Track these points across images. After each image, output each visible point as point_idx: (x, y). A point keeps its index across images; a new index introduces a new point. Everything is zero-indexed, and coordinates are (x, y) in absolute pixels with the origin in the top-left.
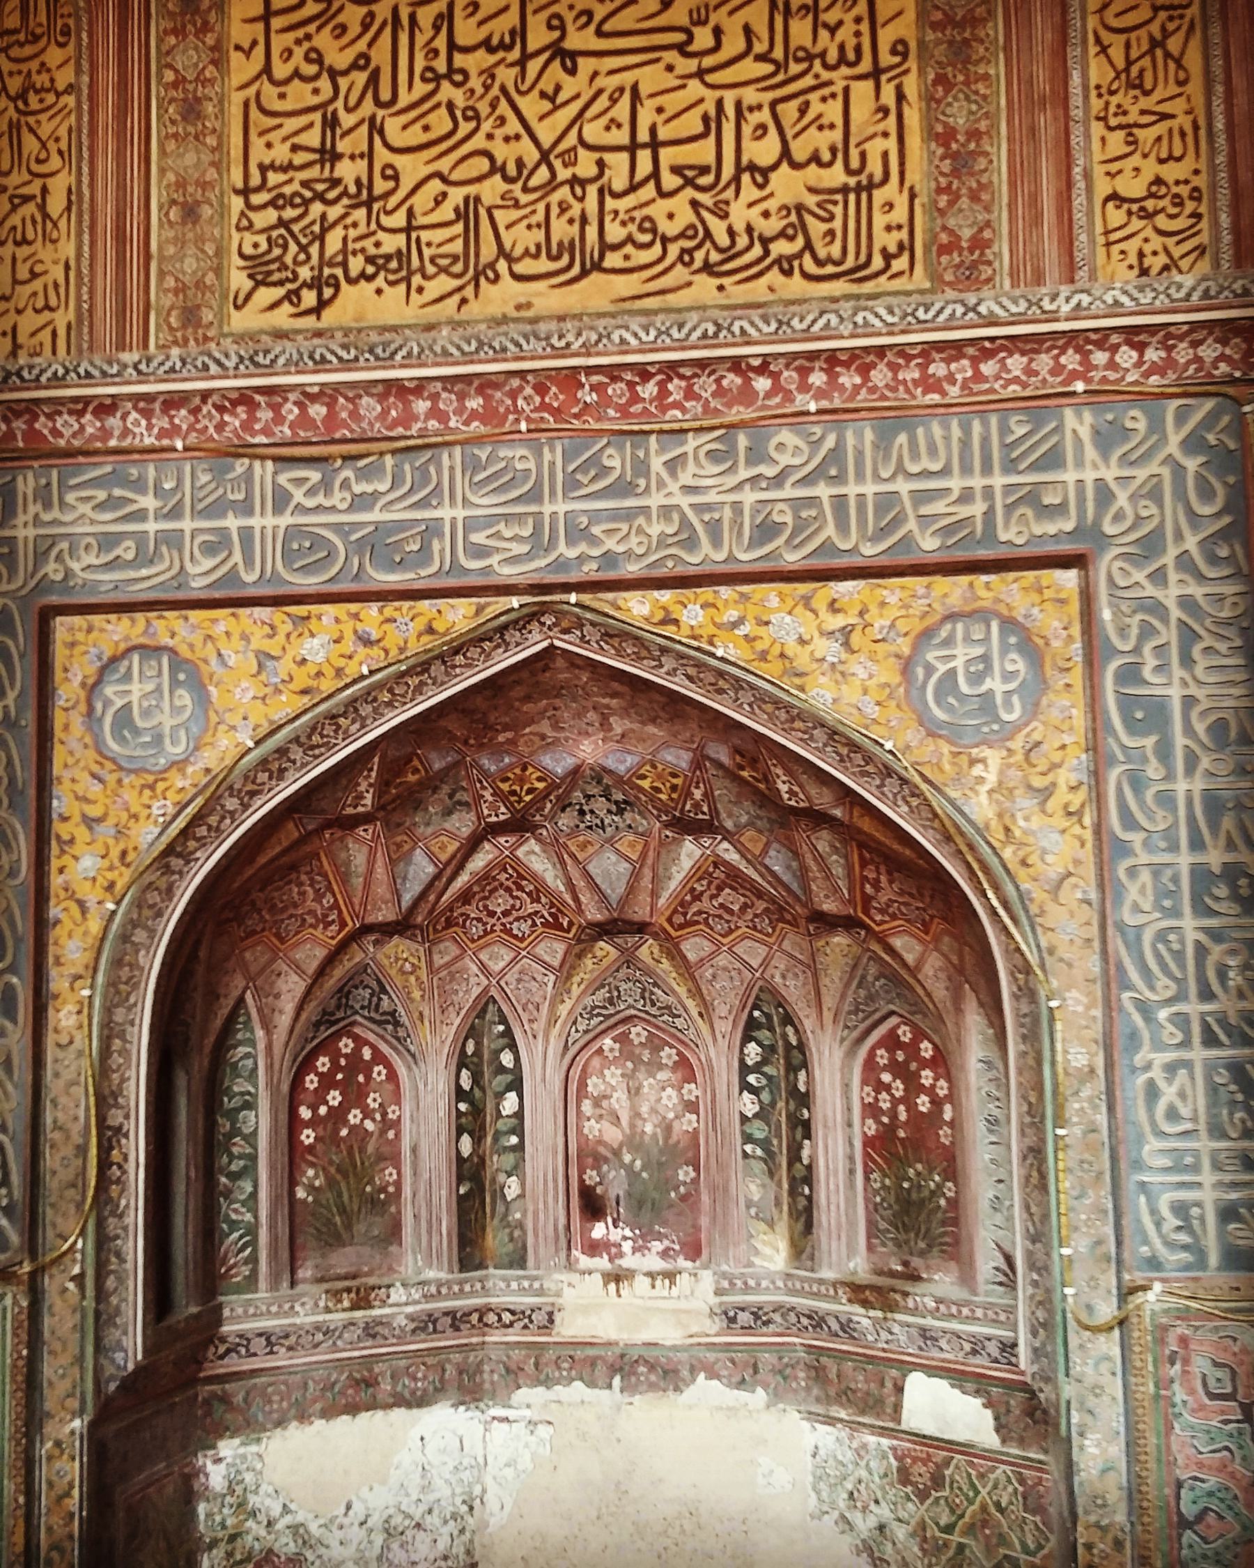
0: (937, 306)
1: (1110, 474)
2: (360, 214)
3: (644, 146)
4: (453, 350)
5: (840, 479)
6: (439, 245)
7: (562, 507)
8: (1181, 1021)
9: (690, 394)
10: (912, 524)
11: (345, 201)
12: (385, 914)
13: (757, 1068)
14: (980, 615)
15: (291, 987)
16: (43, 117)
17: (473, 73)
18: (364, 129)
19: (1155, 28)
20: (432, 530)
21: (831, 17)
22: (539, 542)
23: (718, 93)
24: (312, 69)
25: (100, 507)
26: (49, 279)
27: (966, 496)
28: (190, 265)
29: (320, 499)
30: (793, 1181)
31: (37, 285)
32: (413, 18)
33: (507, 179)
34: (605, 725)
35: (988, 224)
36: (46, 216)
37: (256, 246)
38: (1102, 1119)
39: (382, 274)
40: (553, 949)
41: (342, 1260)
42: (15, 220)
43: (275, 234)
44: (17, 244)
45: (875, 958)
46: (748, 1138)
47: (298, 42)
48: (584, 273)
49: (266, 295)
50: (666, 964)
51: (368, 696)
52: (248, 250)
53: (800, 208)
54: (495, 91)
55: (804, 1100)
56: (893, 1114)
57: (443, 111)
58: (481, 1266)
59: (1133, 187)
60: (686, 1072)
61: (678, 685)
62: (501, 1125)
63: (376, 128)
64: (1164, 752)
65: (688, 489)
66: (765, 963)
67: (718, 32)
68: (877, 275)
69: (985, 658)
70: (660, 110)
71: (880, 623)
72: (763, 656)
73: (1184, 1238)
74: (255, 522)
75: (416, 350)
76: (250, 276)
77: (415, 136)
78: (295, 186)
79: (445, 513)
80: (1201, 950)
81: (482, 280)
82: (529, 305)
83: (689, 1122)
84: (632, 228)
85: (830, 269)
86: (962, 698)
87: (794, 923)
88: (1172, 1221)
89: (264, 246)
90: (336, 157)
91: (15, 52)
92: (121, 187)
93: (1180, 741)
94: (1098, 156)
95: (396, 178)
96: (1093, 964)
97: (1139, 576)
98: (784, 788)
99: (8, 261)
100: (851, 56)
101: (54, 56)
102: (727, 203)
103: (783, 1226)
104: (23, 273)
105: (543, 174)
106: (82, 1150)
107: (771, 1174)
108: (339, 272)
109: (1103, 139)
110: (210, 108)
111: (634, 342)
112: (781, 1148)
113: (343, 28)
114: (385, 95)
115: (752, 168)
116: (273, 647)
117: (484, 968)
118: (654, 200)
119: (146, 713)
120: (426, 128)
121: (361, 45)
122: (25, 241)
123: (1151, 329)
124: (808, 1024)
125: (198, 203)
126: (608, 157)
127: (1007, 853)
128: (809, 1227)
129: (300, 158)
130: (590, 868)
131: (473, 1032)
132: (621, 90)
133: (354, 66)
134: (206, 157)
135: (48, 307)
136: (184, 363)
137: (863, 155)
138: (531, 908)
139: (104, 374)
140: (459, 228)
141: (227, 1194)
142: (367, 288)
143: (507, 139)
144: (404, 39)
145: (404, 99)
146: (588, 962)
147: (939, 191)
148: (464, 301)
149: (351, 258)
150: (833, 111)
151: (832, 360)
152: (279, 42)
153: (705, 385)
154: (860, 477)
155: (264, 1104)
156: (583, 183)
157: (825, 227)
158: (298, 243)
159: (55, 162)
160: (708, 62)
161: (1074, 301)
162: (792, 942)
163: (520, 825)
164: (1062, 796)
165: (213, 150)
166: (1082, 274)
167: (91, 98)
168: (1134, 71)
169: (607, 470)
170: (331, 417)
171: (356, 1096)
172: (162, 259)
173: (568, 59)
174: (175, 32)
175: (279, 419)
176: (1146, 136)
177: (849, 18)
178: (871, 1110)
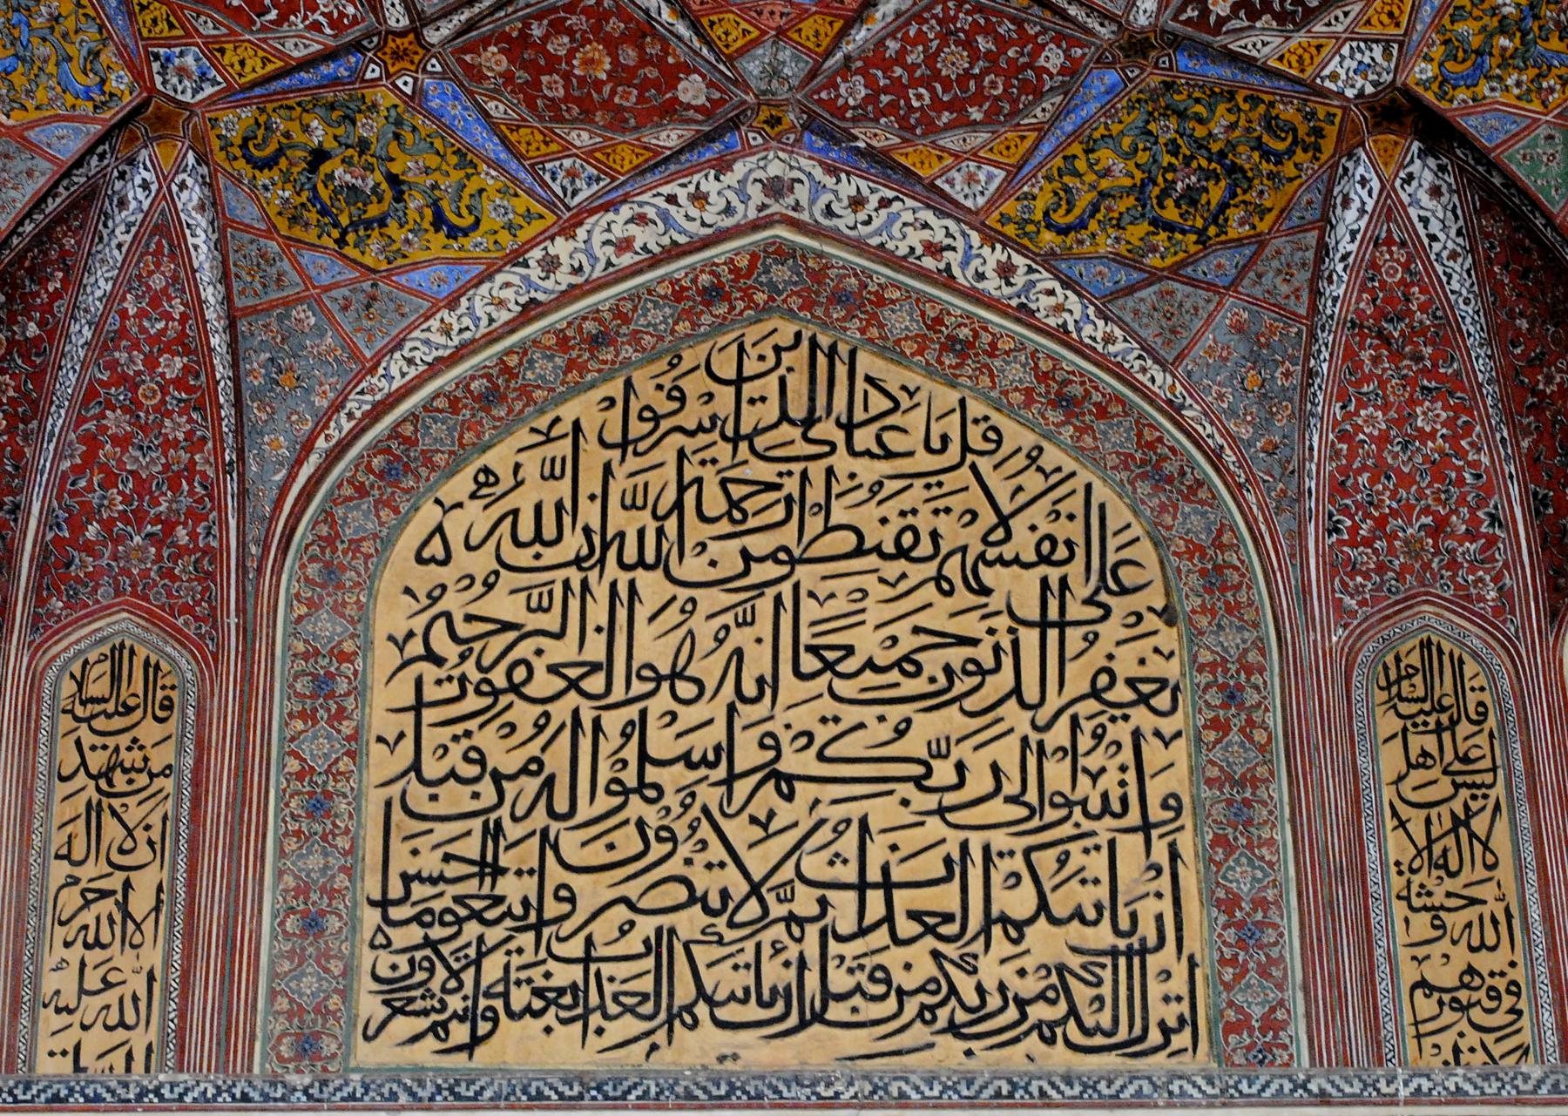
0: (1262, 1080)
2: (527, 939)
3: (875, 886)
4: (699, 1093)
6: (624, 981)
11: (508, 923)
16: (131, 801)
17: (669, 790)
18: (536, 840)
19: (1457, 806)
21: (1092, 762)
23: (963, 835)
24: (472, 771)
26: (127, 991)
28: (309, 984)
31: (111, 997)
32: (597, 723)
33: (708, 911)
35: (1281, 1003)
36: (127, 915)
37: (394, 967)
39: (553, 1009)
42: (88, 917)
43: (418, 955)
44: (87, 946)
47: (456, 738)
48: (803, 1025)
49: (404, 1026)
52: (384, 972)
53: (1061, 969)
54: (695, 811)
57: (631, 829)
59: (1445, 976)
67: (960, 767)
68: (1156, 1050)
70: (894, 848)
75: (653, 1089)
76: (386, 1003)
77: (597, 854)
78: (446, 902)
81: (677, 1023)
82: (735, 1057)
84: (862, 977)
85: (1099, 1040)
89: (404, 969)
90: (498, 871)
91: (99, 724)
92: (234, 889)
94: (1401, 937)
95: (572, 900)
99: (76, 966)
100: (1116, 807)
101: (149, 731)
102: (975, 957)
104: (93, 982)
105: (752, 909)
108: (498, 1004)
109: (1407, 920)
110: (342, 806)
111: (915, 1096)
113: (513, 727)
114: (561, 806)
115: (1004, 920)
118: (888, 947)
120: (611, 847)
121: (533, 749)
122: (98, 944)
125: (322, 913)
126: (832, 895)
132: (848, 822)
133: (524, 770)
134: (336, 861)
135: (122, 1024)
136: (367, 1090)
137: (1134, 917)
139: (266, 1097)
140: (649, 962)
142: (533, 1025)
143: (709, 866)
144: (585, 744)
145: (584, 812)
147: (1223, 962)
148: (654, 1047)
149: (513, 988)
150: (1098, 865)
152: (431, 737)
156: (802, 922)
157: (1094, 992)
158: (448, 967)
159: (143, 854)
160: (950, 799)
161: (1413, 1085)
165: (345, 853)
167: (196, 783)
168: (1437, 849)
172: (274, 975)
173: (786, 784)
174: (302, 715)
176: (1455, 921)
177: (1112, 766)
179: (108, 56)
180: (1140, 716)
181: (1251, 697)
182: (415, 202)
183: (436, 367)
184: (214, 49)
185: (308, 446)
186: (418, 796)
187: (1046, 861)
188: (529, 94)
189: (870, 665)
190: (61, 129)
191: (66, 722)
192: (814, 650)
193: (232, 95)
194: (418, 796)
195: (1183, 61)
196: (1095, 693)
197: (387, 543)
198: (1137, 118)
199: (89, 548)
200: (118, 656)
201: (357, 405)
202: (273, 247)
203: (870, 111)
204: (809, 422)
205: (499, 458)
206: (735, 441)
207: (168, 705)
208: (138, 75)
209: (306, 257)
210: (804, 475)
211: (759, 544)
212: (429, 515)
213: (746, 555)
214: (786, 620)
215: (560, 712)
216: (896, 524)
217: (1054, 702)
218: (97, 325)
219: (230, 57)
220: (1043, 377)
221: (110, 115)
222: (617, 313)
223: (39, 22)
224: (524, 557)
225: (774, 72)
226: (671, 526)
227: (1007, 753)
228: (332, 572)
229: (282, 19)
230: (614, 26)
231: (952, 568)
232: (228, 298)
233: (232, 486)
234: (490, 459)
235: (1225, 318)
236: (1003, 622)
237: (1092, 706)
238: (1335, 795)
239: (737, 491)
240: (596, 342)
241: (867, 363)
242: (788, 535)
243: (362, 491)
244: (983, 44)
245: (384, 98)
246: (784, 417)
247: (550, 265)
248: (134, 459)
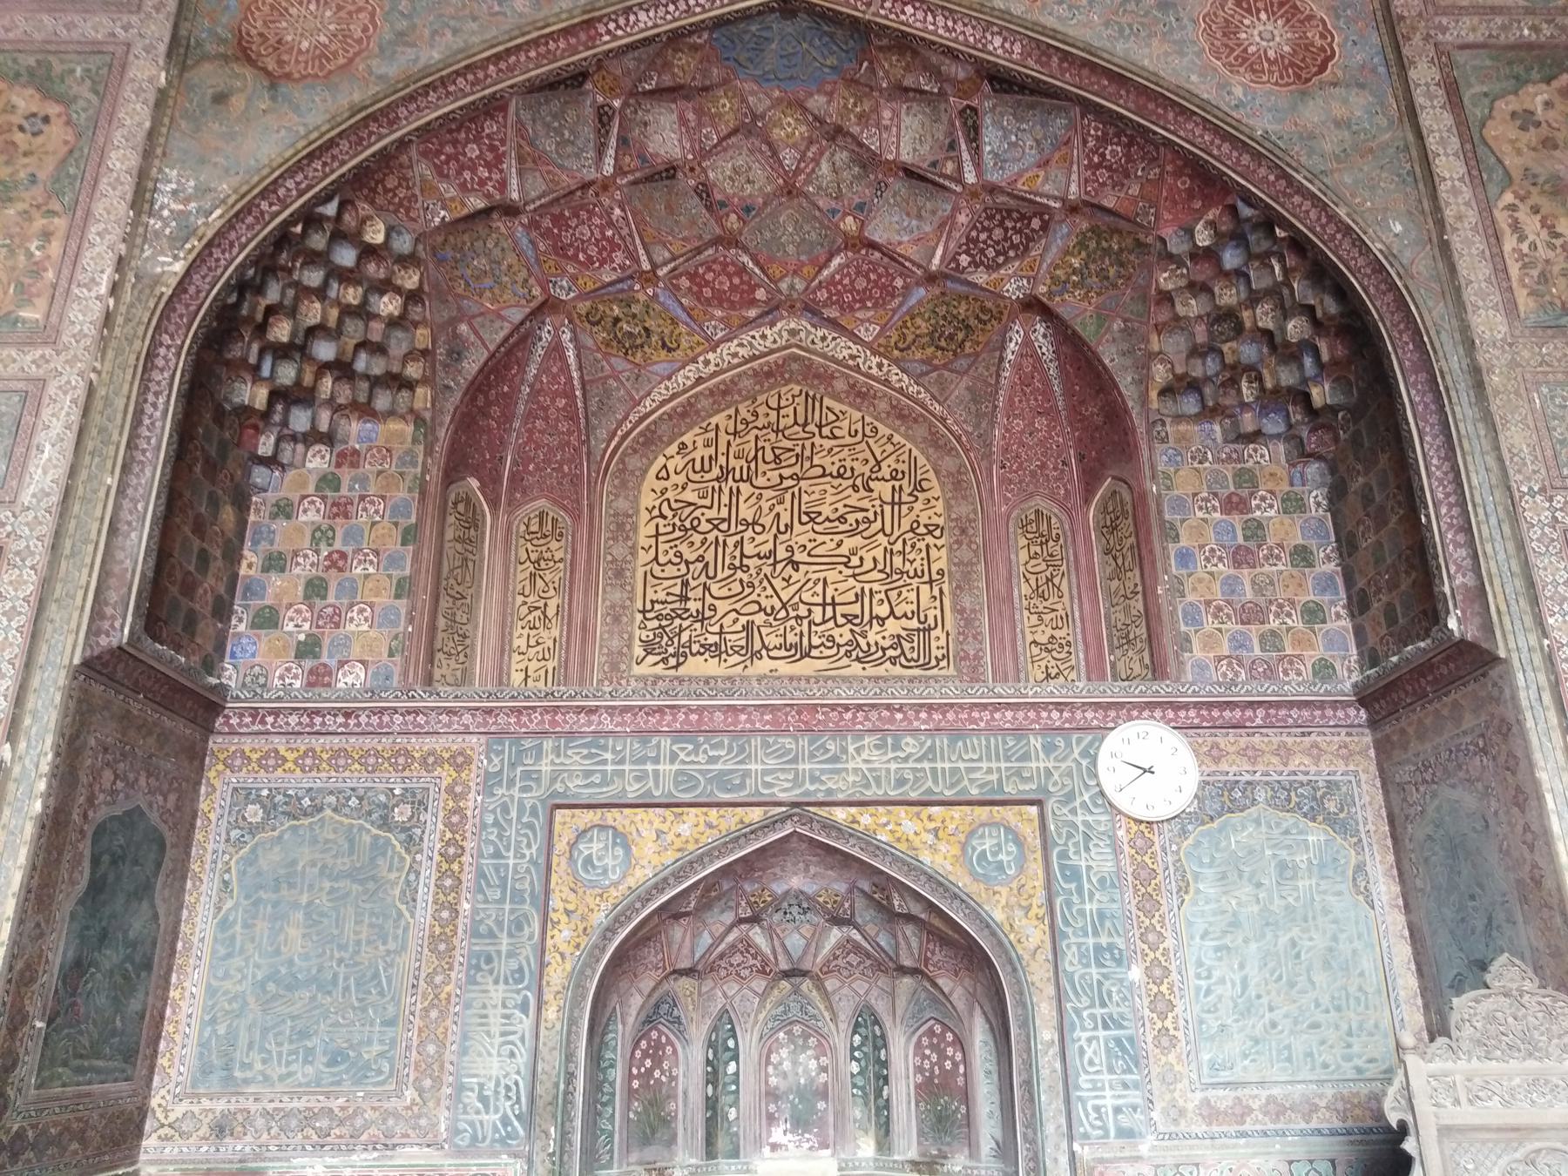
1: (1050, 765)
2: (698, 625)
5: (933, 760)
7: (808, 767)
8: (1093, 1017)
9: (867, 718)
10: (966, 782)
12: (684, 964)
13: (859, 1048)
14: (996, 825)
15: (636, 1001)
20: (747, 774)
21: (911, 557)
22: (797, 781)
25: (585, 757)
27: (990, 771)
29: (692, 758)
30: (878, 1109)
31: (539, 648)
34: (807, 870)
38: (1058, 1065)
40: (760, 984)
41: (650, 1153)
42: (530, 617)
45: (925, 989)
46: (854, 1086)
48: (802, 658)
49: (651, 659)
50: (815, 993)
51: (709, 853)
53: (899, 636)
55: (885, 1064)
56: (932, 1072)
58: (715, 1157)
59: (1043, 639)
60: (821, 1051)
61: (856, 852)
62: (727, 1080)
63: (706, 588)
64: (1080, 890)
65: (866, 761)
66: (867, 993)
67: (861, 559)
69: (999, 845)
71: (952, 827)
72: (898, 840)
73: (1098, 1123)
74: (660, 767)
79: (753, 767)
80: (1100, 983)
83: (823, 1077)
86: (989, 863)
87: (885, 972)
88: (1093, 1115)
92: (586, 607)
93: (1086, 886)
96: (1051, 991)
97: (1065, 811)
98: (896, 903)
101: (554, 545)
103: (872, 1133)
104: (532, 642)
106: (557, 1085)
107: (866, 1104)
112: (871, 1090)
114: (711, 574)
115: (877, 617)
116: (665, 828)
117: (725, 995)
119: (599, 859)
121: (701, 552)
123: (1066, 704)
124: (888, 1024)
127: (1012, 937)
128: (887, 1132)
129: (670, 599)
130: (787, 943)
131: (715, 1029)
134: (625, 595)
138: (752, 962)
141: (600, 1114)
144: (720, 550)
145: (720, 576)
146: (776, 992)
150: (913, 597)
151: (930, 708)
152: (662, 547)
153: (874, 715)
154: (943, 759)
155: (619, 1065)
159: (552, 593)
160: (857, 571)
162: (883, 981)
163: (754, 920)
164: (1035, 910)
166: (1022, 675)
169: (827, 751)
170: (700, 720)
171: (658, 1062)
173: (796, 565)
175: (675, 720)
176: (1047, 618)
178: (919, 1069)
179: (532, 281)
180: (929, 539)
181: (971, 532)
182: (654, 338)
183: (663, 403)
184: (574, 279)
185: (614, 434)
186: (657, 570)
187: (893, 594)
188: (698, 296)
189: (827, 519)
190: (514, 310)
191: (522, 541)
192: (807, 514)
193: (580, 297)
194: (657, 570)
195: (949, 284)
196: (912, 530)
197: (646, 471)
198: (930, 306)
199: (530, 473)
200: (542, 516)
201: (633, 418)
202: (599, 356)
203: (828, 303)
204: (806, 424)
205: (687, 438)
206: (777, 432)
207: (561, 535)
208: (543, 289)
209: (613, 360)
210: (803, 446)
211: (786, 472)
212: (661, 460)
213: (781, 477)
214: (796, 502)
215: (711, 537)
216: (838, 464)
217: (896, 534)
218: (531, 386)
219: (580, 282)
220: (893, 407)
221: (534, 304)
222: (732, 381)
223: (504, 267)
224: (697, 477)
225: (792, 287)
226: (753, 465)
227: (879, 553)
228: (624, 484)
229: (601, 265)
230: (731, 269)
231: (859, 482)
232: (582, 377)
233: (585, 449)
234: (685, 439)
235: (963, 385)
236: (878, 502)
237: (911, 535)
238: (1003, 572)
239: (778, 452)
240: (725, 393)
241: (827, 402)
242: (797, 469)
243: (635, 451)
244: (873, 276)
245: (641, 297)
246: (796, 423)
247: (707, 363)
248: (547, 439)
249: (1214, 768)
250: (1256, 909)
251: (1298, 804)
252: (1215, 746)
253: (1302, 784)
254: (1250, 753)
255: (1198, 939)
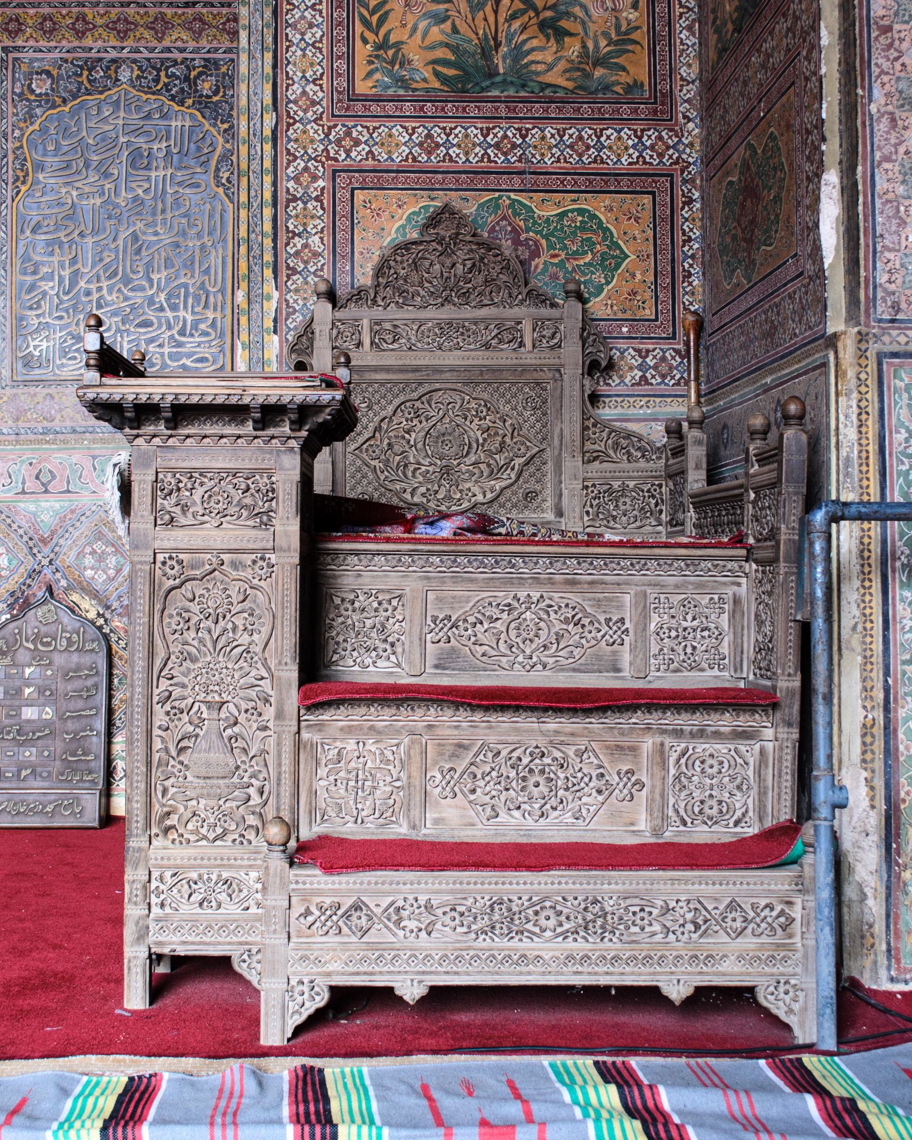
249: (76, 43)
250: (98, 201)
251: (166, 85)
252: (82, 17)
253: (175, 63)
254: (120, 26)
255: (28, 233)
